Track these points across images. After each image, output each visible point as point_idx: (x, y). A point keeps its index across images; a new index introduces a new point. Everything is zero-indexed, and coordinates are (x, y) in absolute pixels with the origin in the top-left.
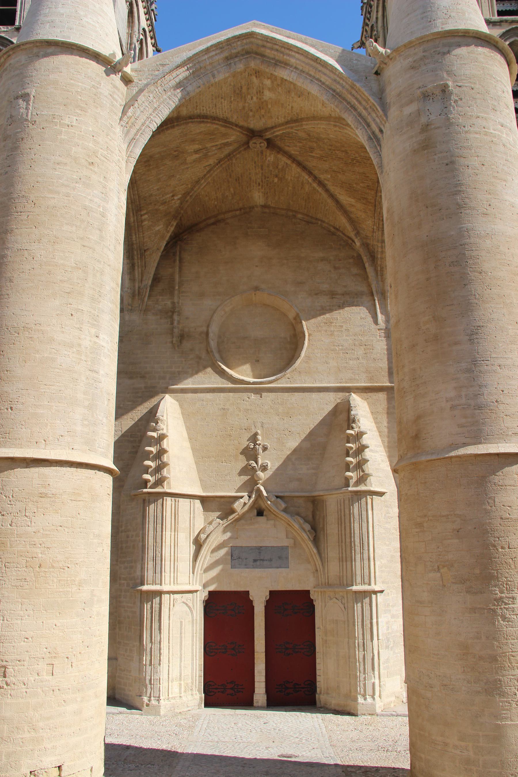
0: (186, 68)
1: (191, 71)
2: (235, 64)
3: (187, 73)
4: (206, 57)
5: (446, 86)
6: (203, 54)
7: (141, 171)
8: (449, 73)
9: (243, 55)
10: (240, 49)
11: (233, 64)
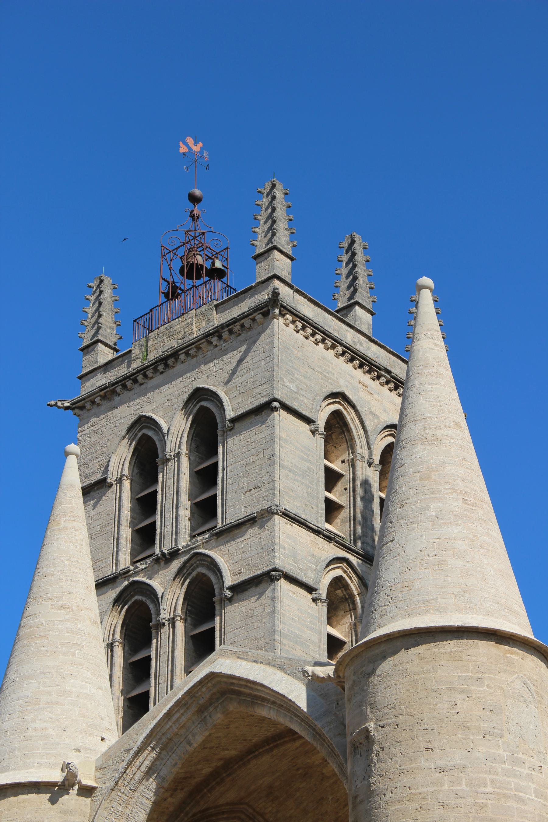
0: (149, 749)
1: (157, 750)
2: (210, 717)
3: (154, 754)
4: (170, 723)
5: (367, 731)
6: (165, 722)
7: (270, 809)
8: (372, 705)
9: (218, 699)
10: (208, 696)
11: (208, 717)
